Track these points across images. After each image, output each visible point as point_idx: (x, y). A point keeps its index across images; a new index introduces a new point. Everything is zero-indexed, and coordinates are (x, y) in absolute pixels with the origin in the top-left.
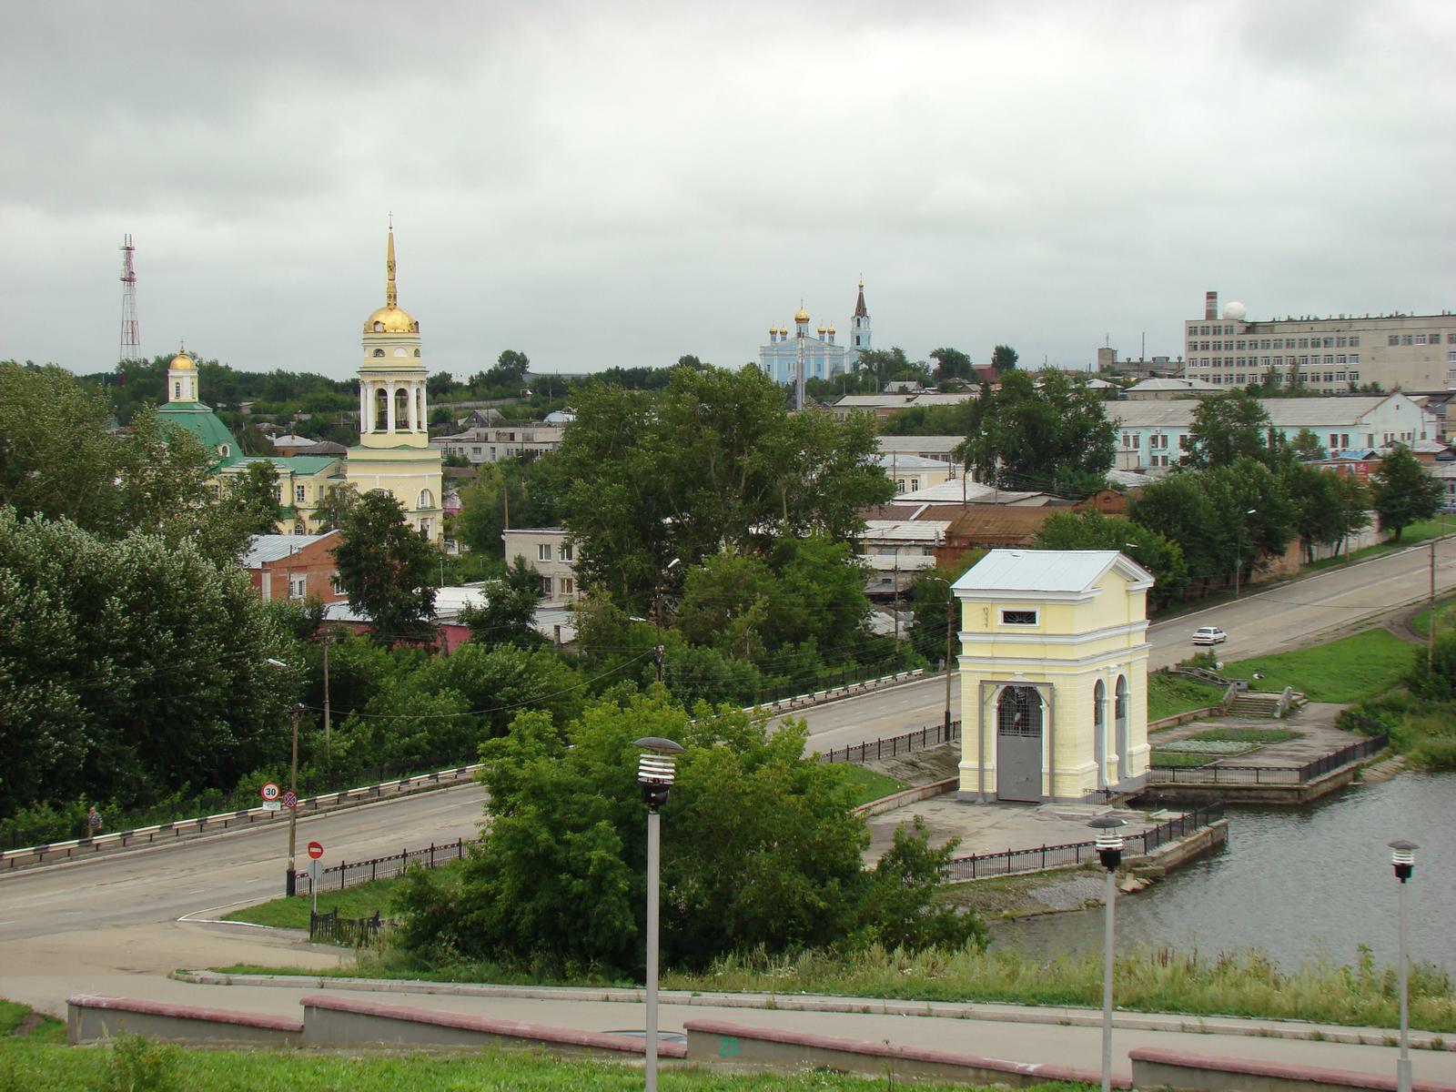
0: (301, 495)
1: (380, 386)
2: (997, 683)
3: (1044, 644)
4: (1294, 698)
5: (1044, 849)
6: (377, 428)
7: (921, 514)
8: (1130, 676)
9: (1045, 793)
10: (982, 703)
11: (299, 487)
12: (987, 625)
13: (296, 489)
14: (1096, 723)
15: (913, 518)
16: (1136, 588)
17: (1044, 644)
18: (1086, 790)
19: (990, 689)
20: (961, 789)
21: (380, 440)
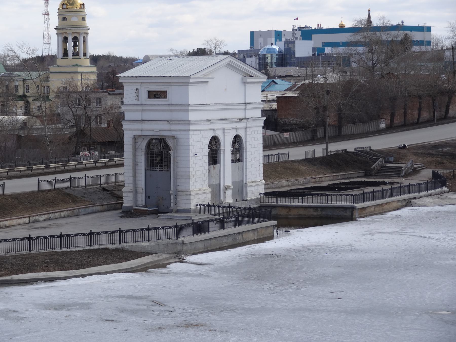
0: (28, 90)
1: (65, 35)
2: (143, 137)
3: (171, 111)
4: (415, 166)
5: (91, 234)
6: (64, 56)
7: (299, 87)
8: (246, 138)
9: (172, 207)
10: (135, 149)
11: (27, 86)
12: (138, 100)
13: (25, 87)
14: (210, 164)
15: (293, 90)
16: (248, 80)
17: (171, 111)
18: (197, 205)
19: (139, 141)
20: (124, 205)
21: (65, 62)
